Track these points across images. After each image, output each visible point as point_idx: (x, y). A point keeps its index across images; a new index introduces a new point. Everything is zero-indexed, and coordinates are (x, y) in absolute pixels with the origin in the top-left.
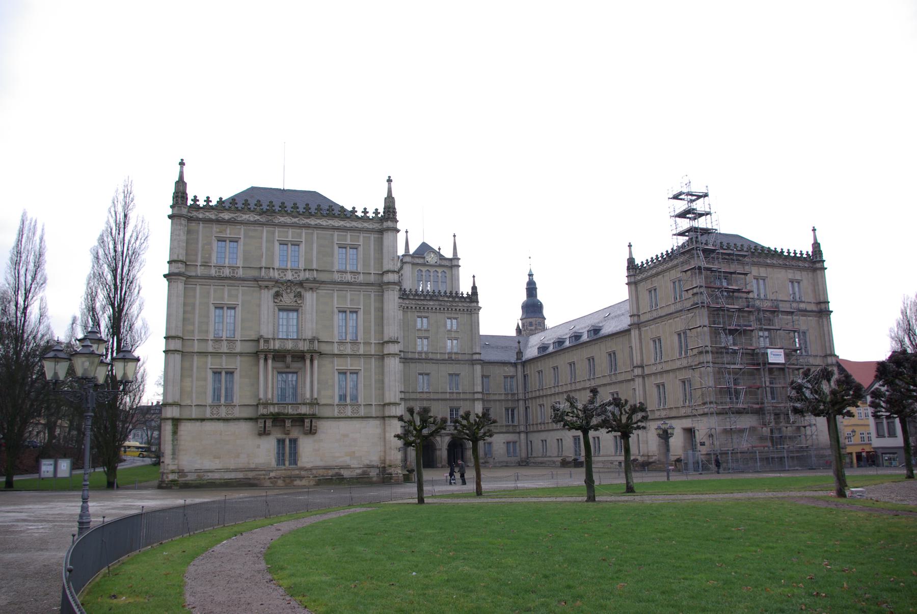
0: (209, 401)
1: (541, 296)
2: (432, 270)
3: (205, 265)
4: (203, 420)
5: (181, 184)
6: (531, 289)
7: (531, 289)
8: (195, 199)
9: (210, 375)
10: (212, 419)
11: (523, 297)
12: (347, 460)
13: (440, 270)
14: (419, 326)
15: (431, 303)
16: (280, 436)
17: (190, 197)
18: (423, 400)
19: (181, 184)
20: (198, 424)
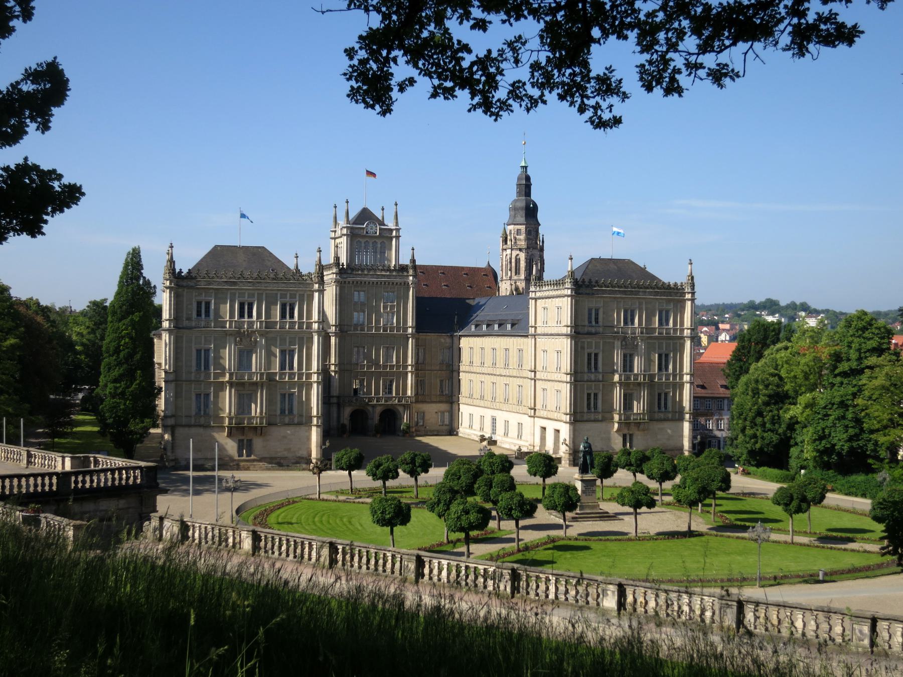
0: (193, 413)
1: (536, 195)
2: (371, 241)
3: (189, 319)
4: (189, 426)
5: (172, 262)
6: (525, 186)
7: (525, 186)
8: (181, 272)
9: (194, 398)
10: (195, 426)
12: (286, 454)
13: (379, 241)
14: (356, 299)
16: (241, 438)
17: (177, 271)
19: (172, 262)
20: (187, 429)
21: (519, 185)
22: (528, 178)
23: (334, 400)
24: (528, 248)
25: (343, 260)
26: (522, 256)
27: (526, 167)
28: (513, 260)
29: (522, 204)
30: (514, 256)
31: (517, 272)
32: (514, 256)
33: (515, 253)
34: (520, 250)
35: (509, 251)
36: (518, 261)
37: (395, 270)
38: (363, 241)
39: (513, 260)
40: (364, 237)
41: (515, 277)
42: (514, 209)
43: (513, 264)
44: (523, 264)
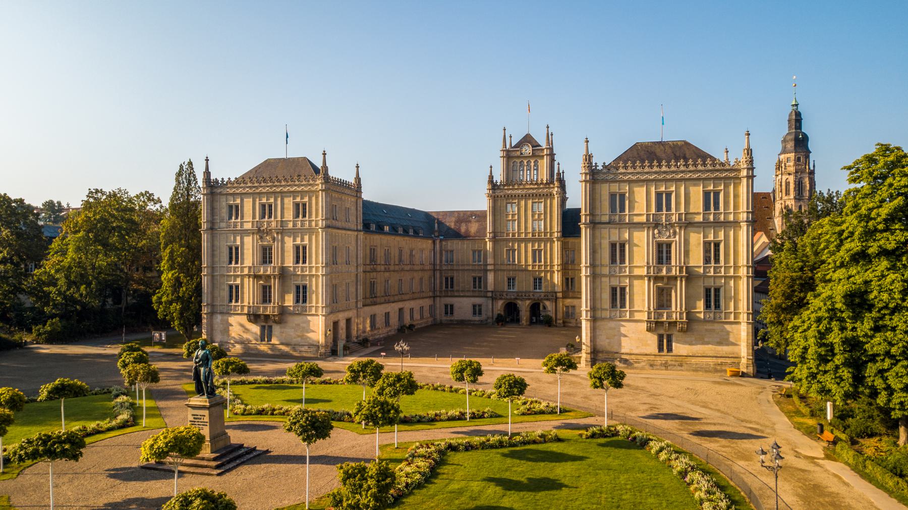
6: (797, 120)
7: (797, 120)
11: (784, 129)
15: (520, 191)
18: (510, 270)
21: (789, 121)
22: (798, 114)
23: (490, 294)
24: (796, 172)
25: (499, 178)
26: (791, 179)
27: (796, 105)
28: (784, 184)
29: (793, 137)
30: (784, 180)
31: (787, 193)
32: (784, 180)
33: (784, 178)
34: (789, 174)
35: (780, 176)
36: (787, 184)
37: (542, 183)
38: (518, 161)
39: (784, 184)
40: (518, 157)
41: (785, 198)
42: (784, 141)
43: (784, 187)
44: (792, 186)
